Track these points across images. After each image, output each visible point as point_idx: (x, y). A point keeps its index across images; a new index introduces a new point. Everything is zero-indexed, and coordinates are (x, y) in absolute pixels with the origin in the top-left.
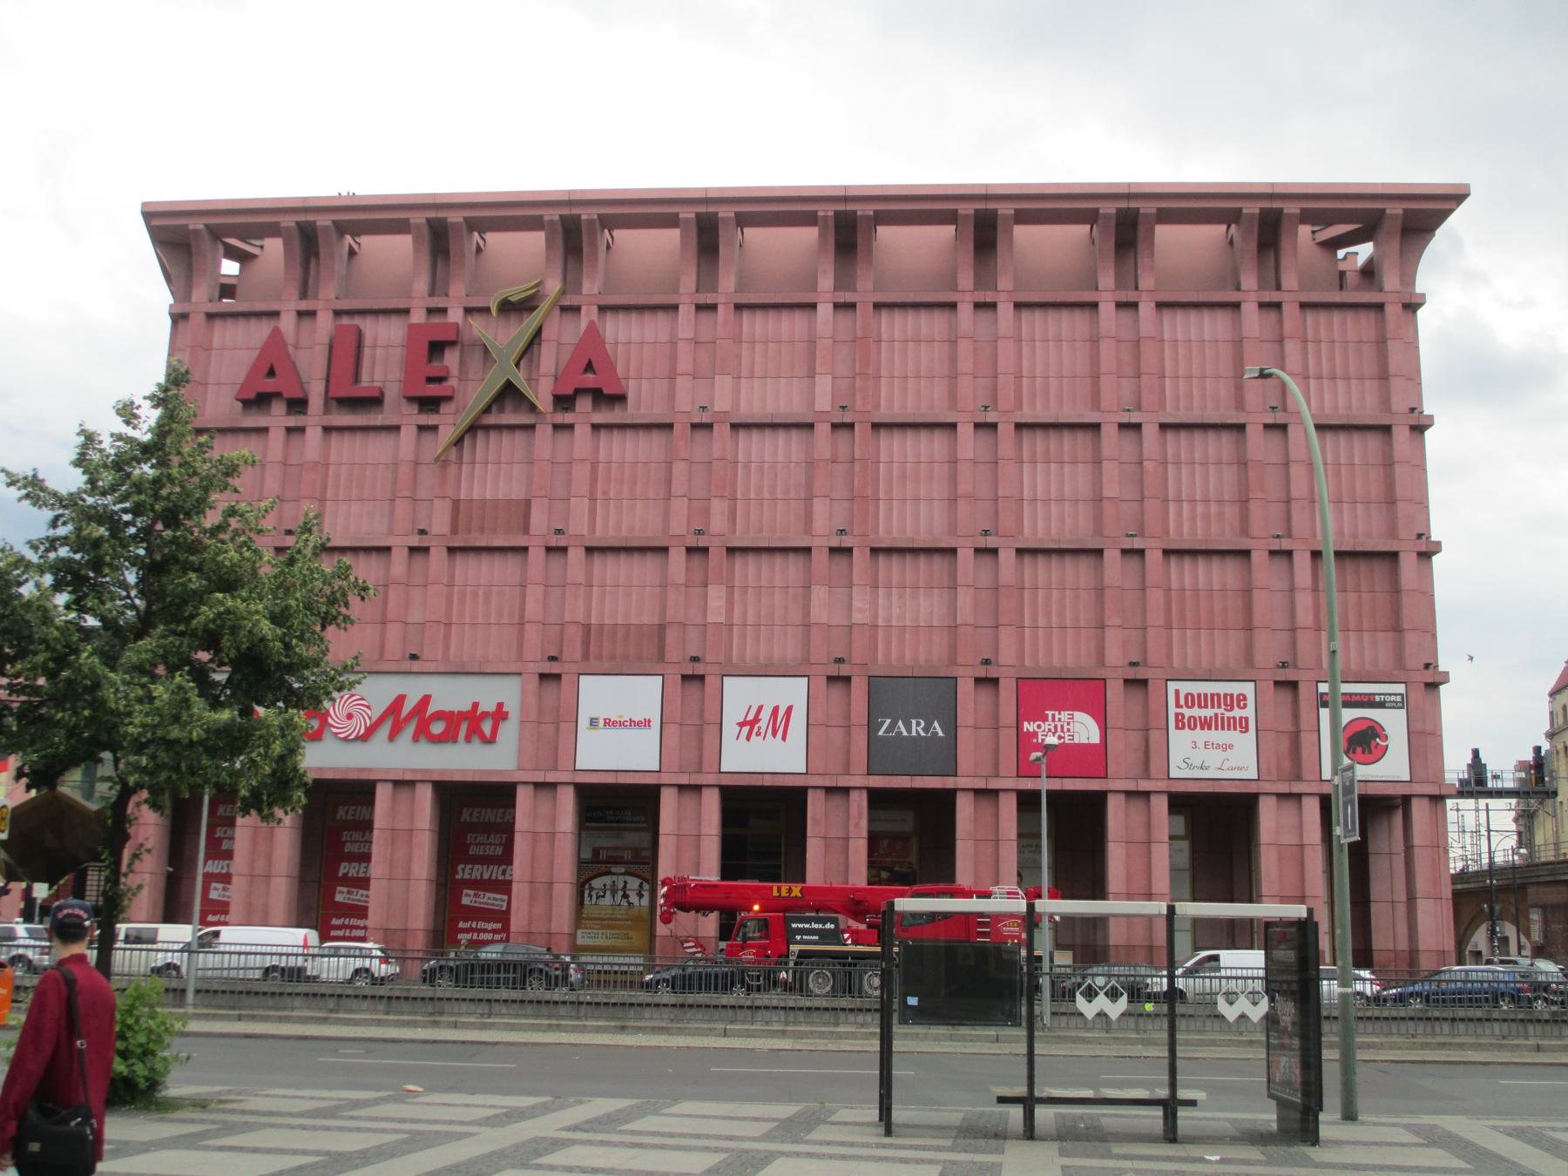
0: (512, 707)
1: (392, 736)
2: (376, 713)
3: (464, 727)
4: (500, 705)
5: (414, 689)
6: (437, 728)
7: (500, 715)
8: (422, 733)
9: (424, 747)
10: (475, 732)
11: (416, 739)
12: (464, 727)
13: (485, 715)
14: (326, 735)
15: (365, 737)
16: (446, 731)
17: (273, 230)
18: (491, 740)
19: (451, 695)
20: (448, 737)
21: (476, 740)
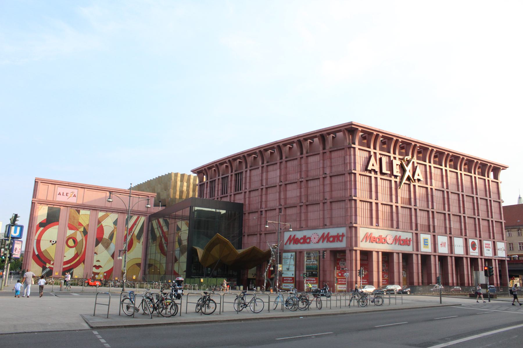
0: (345, 234)
1: (323, 242)
2: (320, 236)
3: (336, 239)
4: (343, 233)
5: (326, 231)
6: (331, 239)
7: (343, 235)
8: (328, 241)
9: (329, 243)
10: (338, 240)
11: (327, 242)
12: (336, 239)
13: (340, 236)
14: (311, 243)
15: (318, 242)
16: (333, 240)
17: (316, 137)
18: (341, 241)
19: (333, 232)
20: (333, 241)
21: (339, 241)
